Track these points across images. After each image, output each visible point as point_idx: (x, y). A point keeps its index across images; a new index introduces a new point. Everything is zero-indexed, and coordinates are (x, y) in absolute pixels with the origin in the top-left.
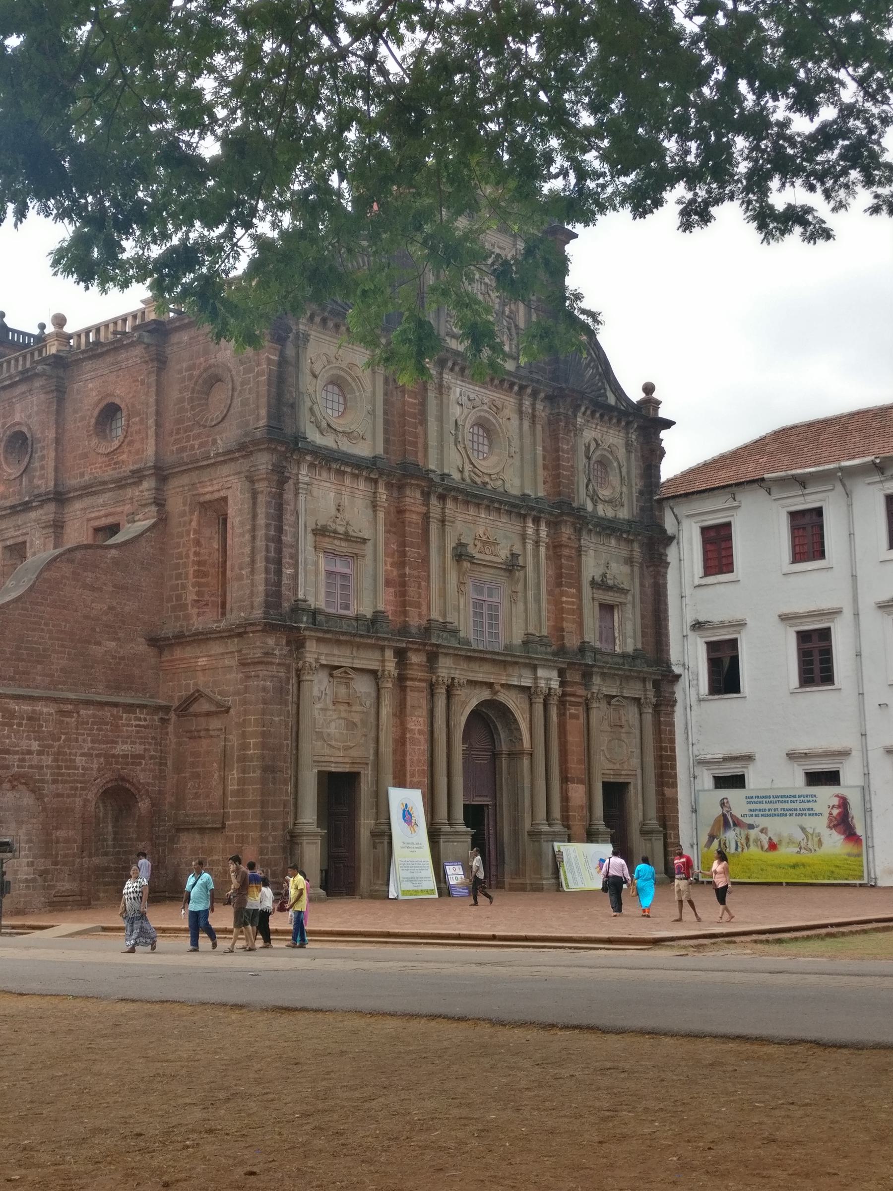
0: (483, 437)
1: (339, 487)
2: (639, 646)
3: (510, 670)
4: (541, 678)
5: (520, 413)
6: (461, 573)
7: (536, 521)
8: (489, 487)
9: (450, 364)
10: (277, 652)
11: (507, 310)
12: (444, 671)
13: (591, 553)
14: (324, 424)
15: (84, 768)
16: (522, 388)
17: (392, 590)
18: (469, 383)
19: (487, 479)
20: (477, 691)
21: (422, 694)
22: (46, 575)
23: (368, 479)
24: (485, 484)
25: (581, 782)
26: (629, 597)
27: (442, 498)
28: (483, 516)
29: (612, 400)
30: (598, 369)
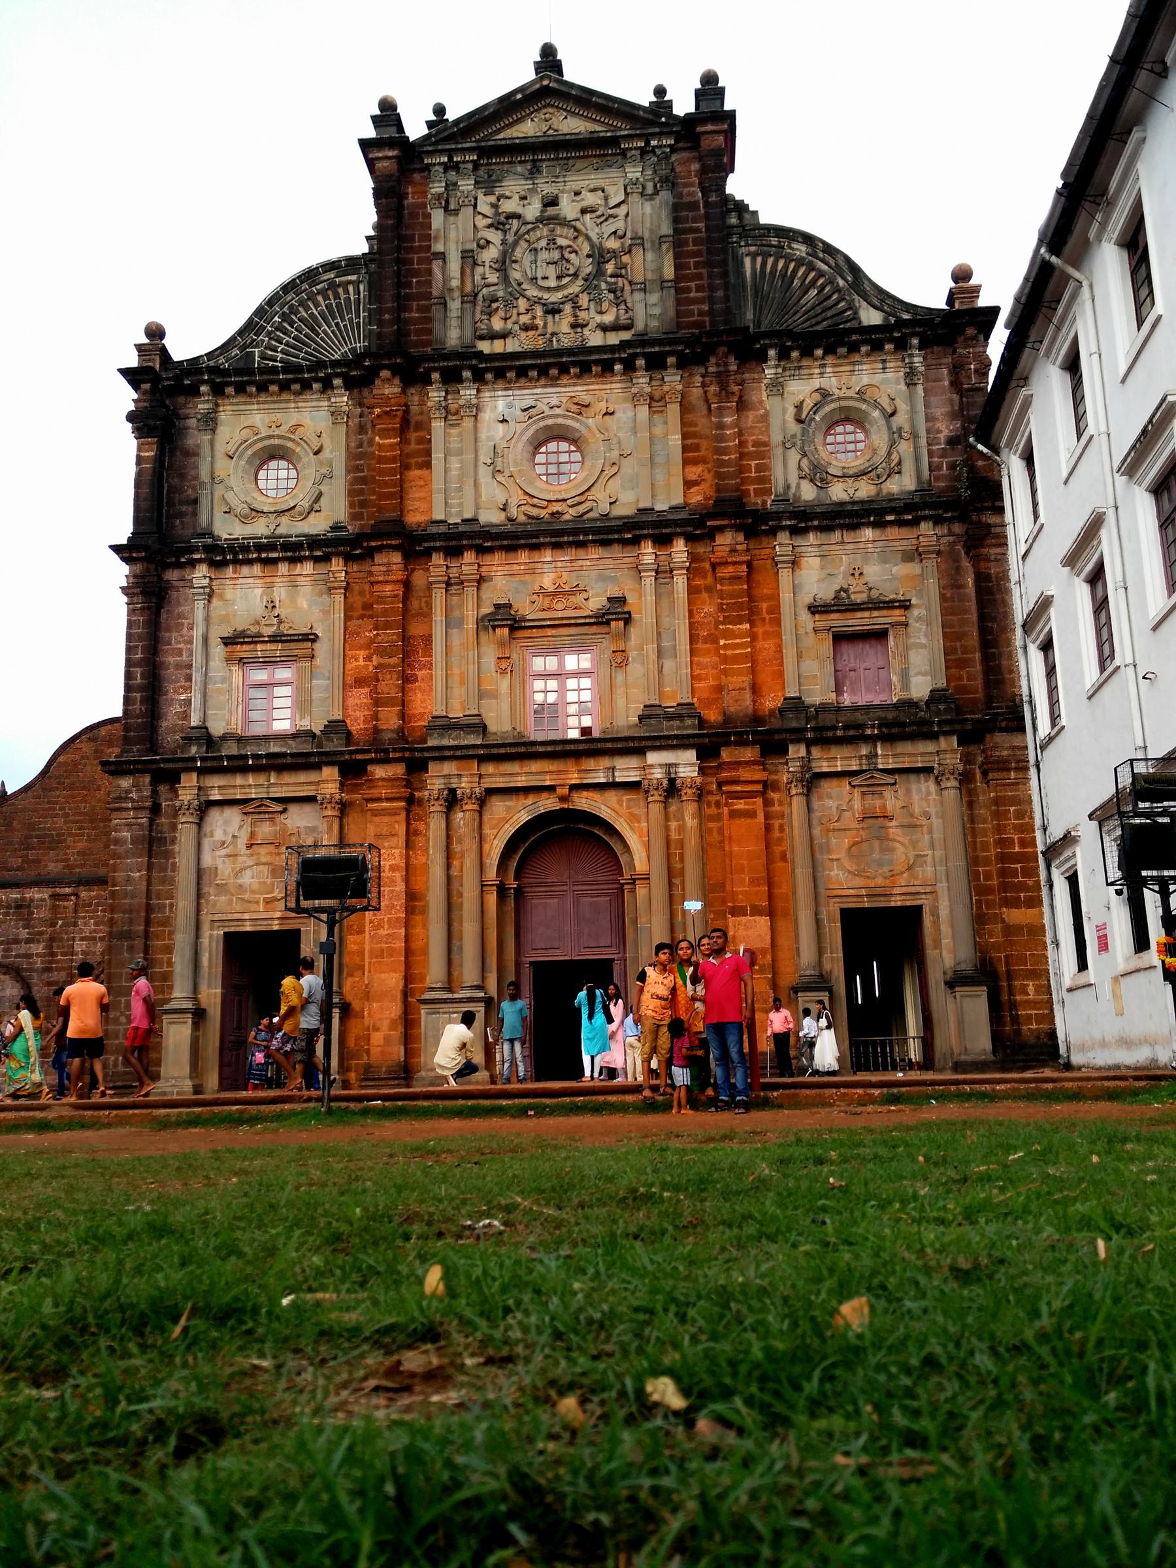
0: (570, 452)
1: (269, 580)
2: (942, 683)
3: (590, 763)
4: (652, 766)
5: (635, 399)
6: (501, 644)
7: (662, 541)
8: (567, 517)
9: (467, 374)
10: (134, 795)
11: (610, 268)
12: (437, 781)
13: (815, 562)
14: (240, 508)
15: (84, 952)
16: (629, 367)
17: (367, 690)
18: (520, 388)
19: (557, 507)
20: (530, 801)
21: (397, 818)
22: (61, 759)
23: (317, 560)
24: (553, 514)
25: (756, 911)
26: (915, 612)
27: (454, 552)
28: (549, 559)
29: (871, 317)
30: (831, 282)
